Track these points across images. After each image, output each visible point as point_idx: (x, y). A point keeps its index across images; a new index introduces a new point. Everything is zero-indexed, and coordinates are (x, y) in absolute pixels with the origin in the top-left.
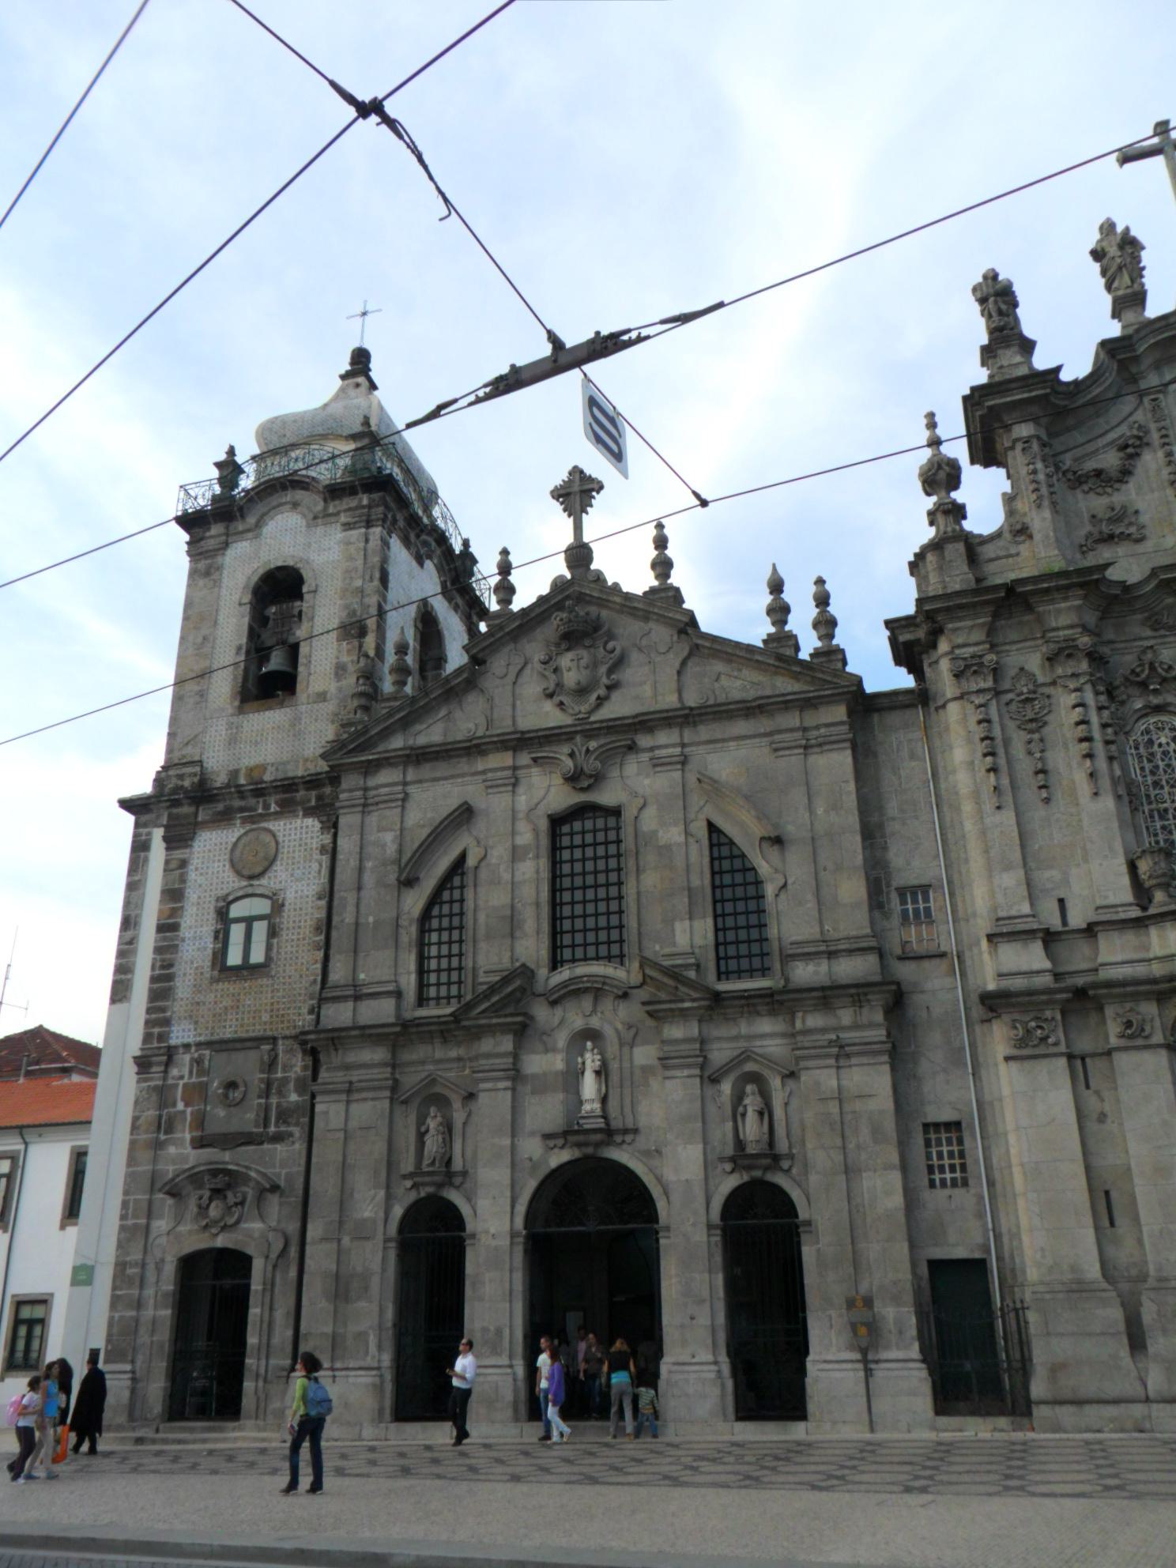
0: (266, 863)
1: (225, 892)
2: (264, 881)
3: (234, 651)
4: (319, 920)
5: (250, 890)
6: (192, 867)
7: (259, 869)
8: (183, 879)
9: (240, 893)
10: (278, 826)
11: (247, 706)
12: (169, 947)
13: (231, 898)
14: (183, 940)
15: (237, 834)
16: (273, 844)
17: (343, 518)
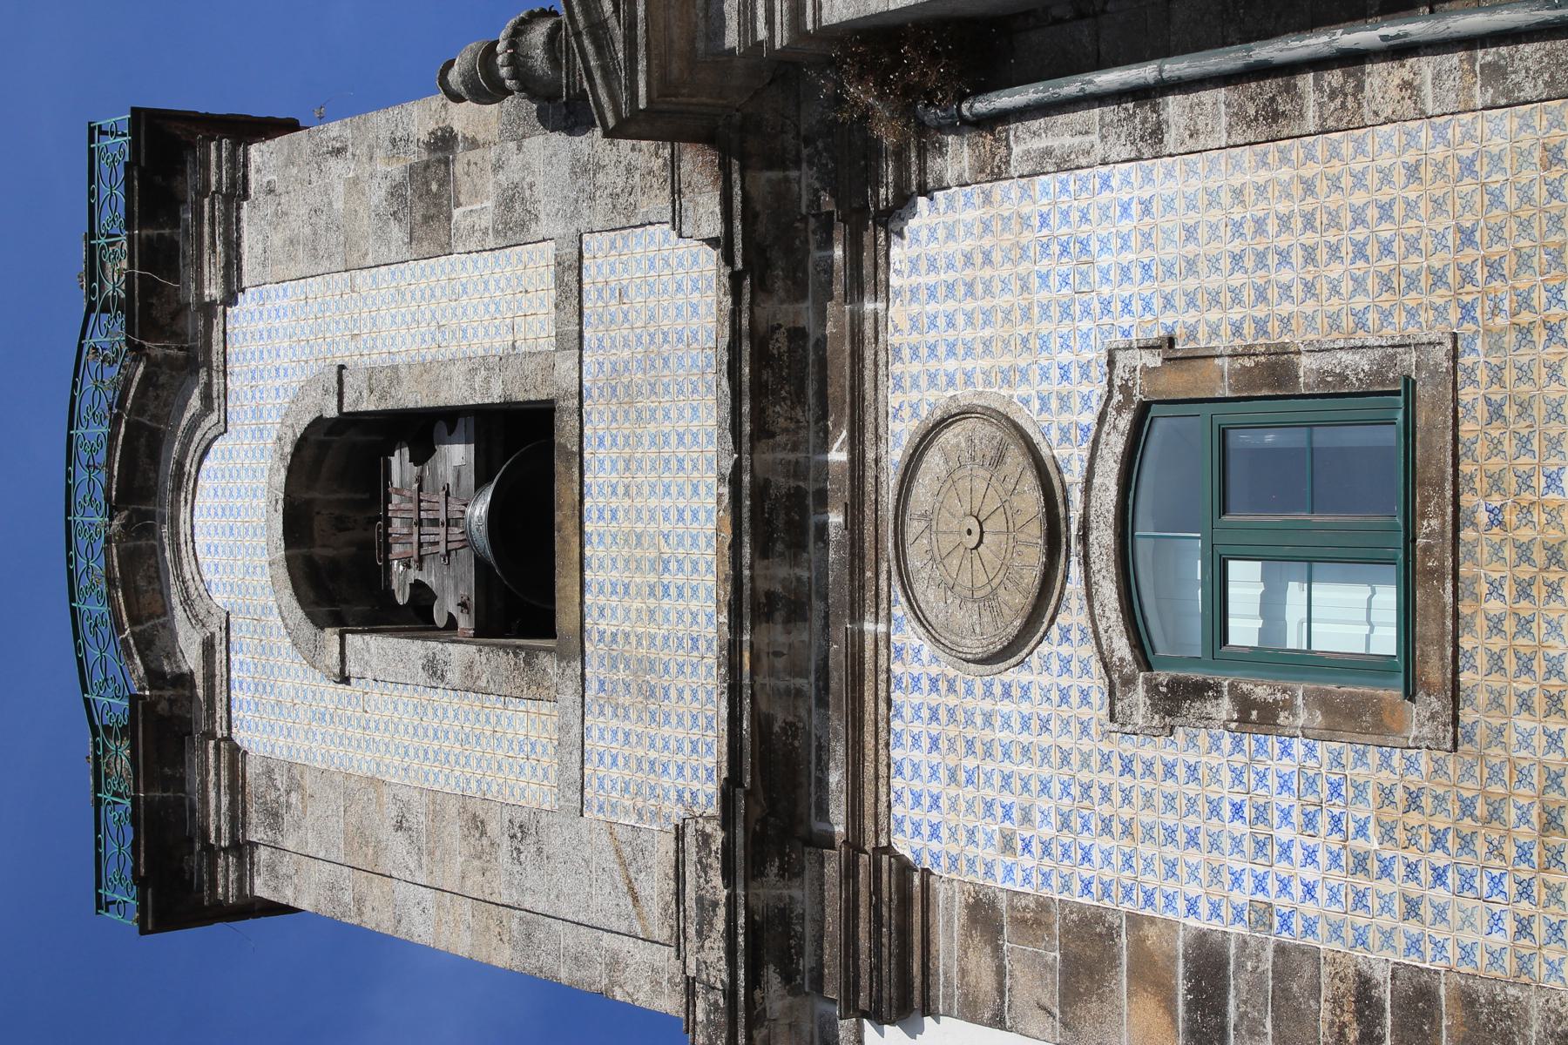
0: (1016, 458)
1: (1096, 683)
2: (1071, 460)
3: (441, 697)
4: (1239, 116)
5: (1103, 537)
6: (998, 882)
7: (1031, 500)
8: (1035, 918)
9: (1108, 591)
10: (904, 402)
11: (565, 620)
12: (1282, 996)
13: (1121, 647)
14: (1262, 915)
15: (908, 635)
16: (949, 437)
17: (213, 291)
